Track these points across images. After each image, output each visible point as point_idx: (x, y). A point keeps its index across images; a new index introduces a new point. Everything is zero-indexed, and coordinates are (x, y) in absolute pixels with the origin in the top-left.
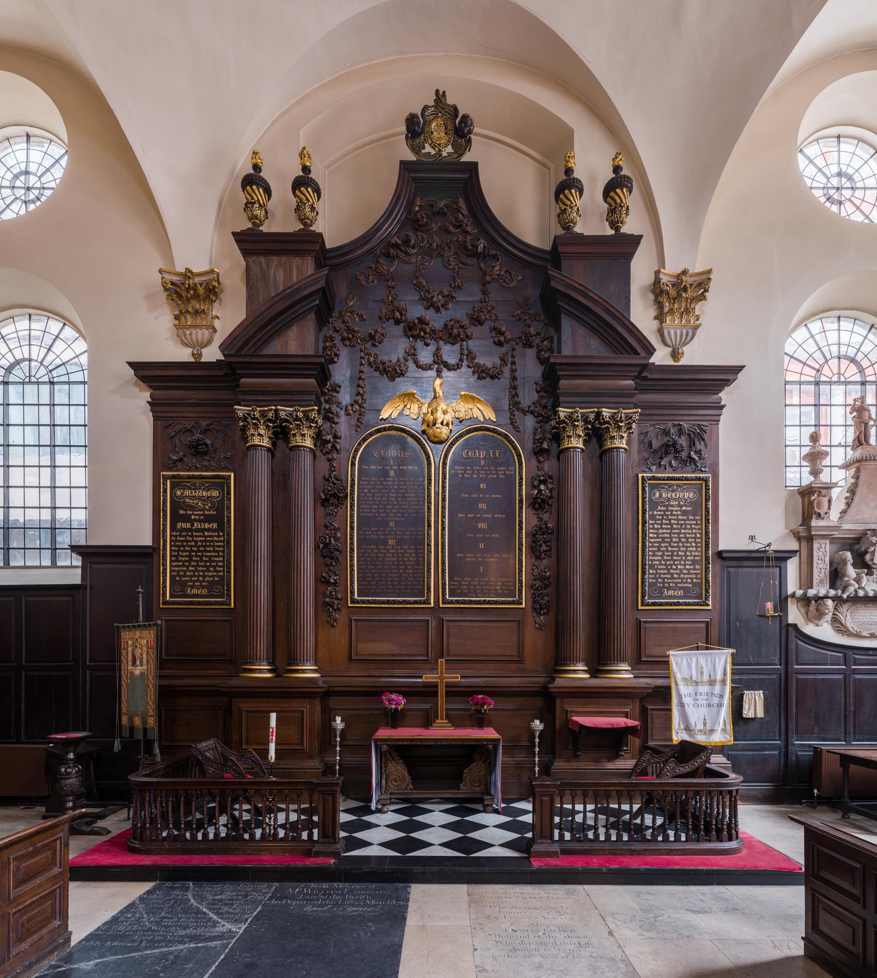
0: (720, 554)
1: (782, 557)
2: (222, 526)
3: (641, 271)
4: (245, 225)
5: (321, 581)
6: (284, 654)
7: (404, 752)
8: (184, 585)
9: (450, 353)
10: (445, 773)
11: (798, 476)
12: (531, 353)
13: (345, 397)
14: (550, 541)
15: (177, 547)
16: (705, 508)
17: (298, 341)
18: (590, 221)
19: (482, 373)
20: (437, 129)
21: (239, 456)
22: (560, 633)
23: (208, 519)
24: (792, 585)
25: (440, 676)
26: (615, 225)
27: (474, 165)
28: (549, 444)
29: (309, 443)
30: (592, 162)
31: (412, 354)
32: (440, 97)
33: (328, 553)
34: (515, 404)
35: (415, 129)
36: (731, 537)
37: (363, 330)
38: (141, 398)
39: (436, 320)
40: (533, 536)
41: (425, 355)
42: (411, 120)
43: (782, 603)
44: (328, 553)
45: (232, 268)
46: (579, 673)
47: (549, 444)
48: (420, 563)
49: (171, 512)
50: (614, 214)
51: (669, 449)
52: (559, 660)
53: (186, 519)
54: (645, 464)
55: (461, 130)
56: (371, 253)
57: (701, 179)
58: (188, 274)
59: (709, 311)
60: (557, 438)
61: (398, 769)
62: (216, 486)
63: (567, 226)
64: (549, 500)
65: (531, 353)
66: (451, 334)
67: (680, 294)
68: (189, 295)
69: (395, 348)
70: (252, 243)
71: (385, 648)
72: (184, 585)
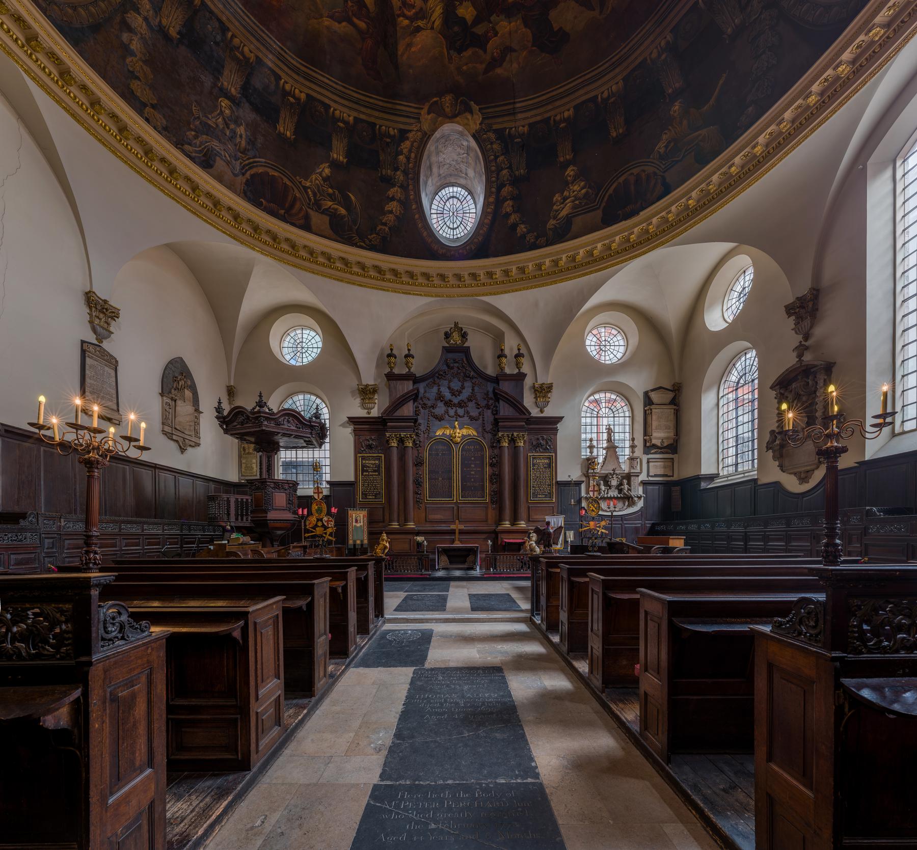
0: (557, 483)
1: (578, 484)
3: (528, 382)
4: (387, 370)
7: (446, 551)
8: (366, 495)
9: (461, 411)
10: (461, 558)
11: (586, 453)
12: (489, 411)
13: (423, 428)
14: (497, 478)
16: (551, 465)
17: (408, 410)
19: (472, 418)
21: (387, 449)
22: (501, 510)
23: (375, 471)
24: (583, 494)
25: (457, 526)
26: (519, 368)
28: (495, 444)
29: (411, 445)
30: (510, 344)
31: (447, 412)
35: (447, 336)
36: (562, 477)
37: (429, 403)
38: (349, 430)
39: (456, 401)
40: (491, 477)
41: (452, 412)
43: (579, 501)
44: (418, 483)
45: (382, 383)
46: (507, 525)
47: (495, 444)
48: (451, 486)
49: (361, 469)
50: (518, 365)
51: (539, 445)
52: (500, 520)
53: (367, 471)
54: (530, 450)
55: (464, 336)
56: (433, 377)
58: (367, 386)
59: (554, 396)
60: (499, 441)
61: (444, 558)
62: (377, 459)
63: (502, 369)
64: (496, 464)
65: (489, 411)
66: (461, 405)
67: (543, 392)
68: (366, 393)
69: (440, 409)
71: (438, 517)
72: (366, 495)
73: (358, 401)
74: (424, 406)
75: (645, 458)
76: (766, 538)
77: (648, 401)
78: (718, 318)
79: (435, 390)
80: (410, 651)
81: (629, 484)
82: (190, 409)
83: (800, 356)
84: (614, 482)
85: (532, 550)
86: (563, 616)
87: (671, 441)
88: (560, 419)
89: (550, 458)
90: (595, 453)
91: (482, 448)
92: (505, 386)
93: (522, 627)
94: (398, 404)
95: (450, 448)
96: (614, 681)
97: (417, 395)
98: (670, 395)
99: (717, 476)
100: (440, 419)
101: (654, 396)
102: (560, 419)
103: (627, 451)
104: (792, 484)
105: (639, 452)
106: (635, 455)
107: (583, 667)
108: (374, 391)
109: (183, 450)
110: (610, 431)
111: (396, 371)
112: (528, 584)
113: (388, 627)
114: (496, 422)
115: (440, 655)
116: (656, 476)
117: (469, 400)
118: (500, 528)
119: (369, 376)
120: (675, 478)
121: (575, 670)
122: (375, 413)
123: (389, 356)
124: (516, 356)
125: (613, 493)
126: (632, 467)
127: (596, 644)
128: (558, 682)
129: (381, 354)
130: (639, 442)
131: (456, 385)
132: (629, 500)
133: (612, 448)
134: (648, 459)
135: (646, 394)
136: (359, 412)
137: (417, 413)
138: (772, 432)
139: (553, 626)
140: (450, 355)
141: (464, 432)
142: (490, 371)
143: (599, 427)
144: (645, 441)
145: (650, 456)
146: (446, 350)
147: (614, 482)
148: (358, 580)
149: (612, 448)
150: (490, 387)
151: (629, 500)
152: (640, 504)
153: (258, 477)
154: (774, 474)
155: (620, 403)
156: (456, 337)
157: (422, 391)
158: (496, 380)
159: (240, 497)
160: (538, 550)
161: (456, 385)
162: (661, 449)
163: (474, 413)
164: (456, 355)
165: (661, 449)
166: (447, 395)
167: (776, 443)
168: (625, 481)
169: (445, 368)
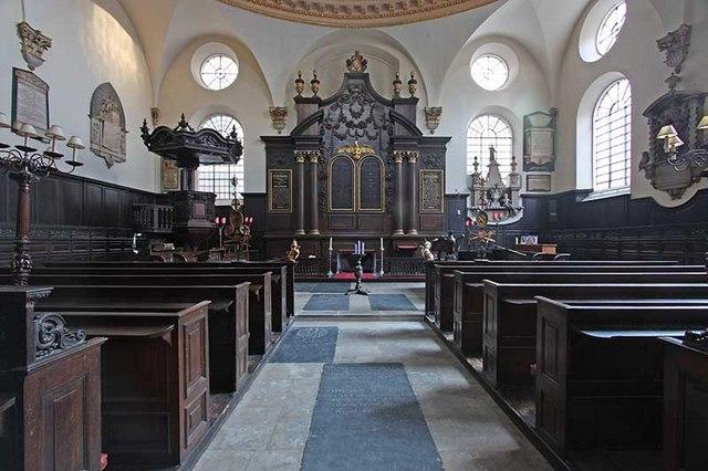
1: (465, 196)
3: (420, 106)
5: (320, 204)
6: (309, 228)
9: (360, 132)
11: (471, 170)
13: (327, 146)
14: (392, 192)
16: (441, 181)
17: (314, 130)
19: (370, 138)
20: (356, 63)
24: (469, 206)
28: (391, 161)
30: (404, 77)
31: (348, 132)
32: (357, 53)
33: (322, 195)
34: (381, 148)
35: (349, 63)
37: (333, 124)
39: (356, 122)
40: (386, 190)
41: (352, 132)
42: (348, 61)
44: (322, 195)
46: (401, 233)
49: (271, 182)
52: (395, 228)
55: (364, 64)
56: (336, 101)
57: (438, 83)
58: (278, 108)
59: (443, 118)
60: (394, 159)
63: (397, 93)
64: (392, 178)
68: (278, 115)
70: (299, 100)
73: (270, 121)
74: (329, 127)
75: (524, 174)
76: (639, 247)
77: (527, 124)
78: (595, 46)
79: (338, 112)
80: (318, 349)
81: (510, 197)
82: (117, 129)
83: (672, 87)
84: (496, 196)
85: (427, 256)
86: (458, 317)
89: (439, 174)
90: (479, 171)
91: (379, 164)
92: (401, 110)
93: (417, 326)
94: (304, 124)
95: (351, 164)
96: (507, 383)
97: (322, 116)
98: (548, 119)
99: (592, 191)
100: (342, 138)
101: (533, 120)
103: (509, 169)
104: (664, 200)
105: (519, 169)
106: (516, 172)
107: (478, 364)
108: (285, 114)
109: (109, 165)
110: (492, 151)
112: (423, 285)
113: (296, 325)
114: (392, 141)
115: (344, 351)
116: (534, 190)
117: (368, 121)
118: (395, 235)
119: (279, 103)
120: (552, 192)
121: (470, 367)
122: (286, 133)
123: (297, 81)
124: (410, 82)
125: (496, 205)
126: (512, 182)
127: (490, 344)
128: (454, 378)
129: (289, 83)
130: (519, 160)
131: (356, 108)
132: (510, 211)
133: (494, 165)
135: (525, 117)
137: (322, 132)
138: (645, 154)
139: (447, 325)
140: (351, 81)
141: (364, 150)
142: (388, 97)
143: (482, 147)
144: (524, 159)
145: (529, 173)
146: (348, 76)
147: (496, 196)
148: (273, 282)
149: (494, 165)
150: (387, 110)
151: (510, 211)
152: (520, 215)
153: (179, 189)
154: (647, 190)
155: (502, 125)
156: (356, 63)
157: (326, 113)
158: (392, 104)
159: (162, 207)
160: (432, 256)
161: (356, 108)
162: (539, 167)
163: (372, 133)
164: (358, 84)
165: (539, 167)
166: (349, 118)
167: (651, 160)
168: (506, 195)
169: (347, 92)
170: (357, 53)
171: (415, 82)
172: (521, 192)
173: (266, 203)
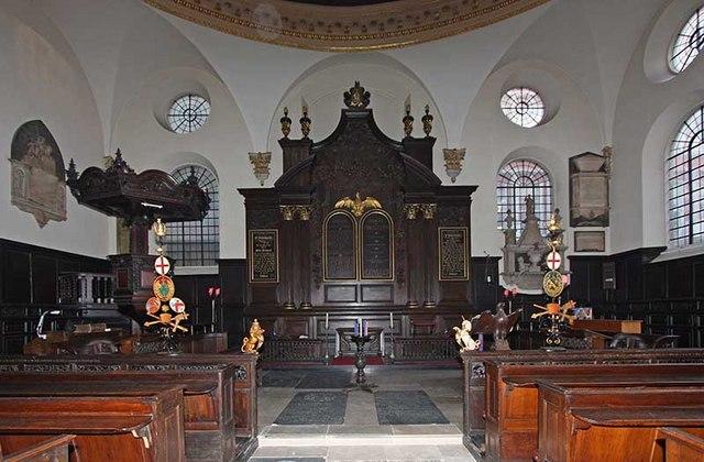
2: (272, 247)
3: (437, 151)
15: (256, 259)
16: (464, 240)
18: (418, 133)
20: (356, 96)
23: (268, 248)
26: (427, 133)
27: (371, 111)
32: (357, 84)
42: (346, 94)
45: (278, 154)
49: (253, 244)
50: (427, 128)
55: (366, 97)
62: (272, 235)
67: (454, 158)
68: (260, 163)
70: (284, 143)
87: (603, 213)
88: (474, 188)
98: (600, 162)
99: (664, 249)
101: (581, 164)
102: (474, 188)
109: (42, 224)
111: (291, 137)
119: (260, 148)
120: (608, 252)
122: (270, 184)
134: (575, 233)
135: (571, 159)
136: (254, 183)
145: (578, 229)
159: (99, 277)
170: (357, 84)
171: (431, 118)
172: (567, 254)
173: (246, 274)
